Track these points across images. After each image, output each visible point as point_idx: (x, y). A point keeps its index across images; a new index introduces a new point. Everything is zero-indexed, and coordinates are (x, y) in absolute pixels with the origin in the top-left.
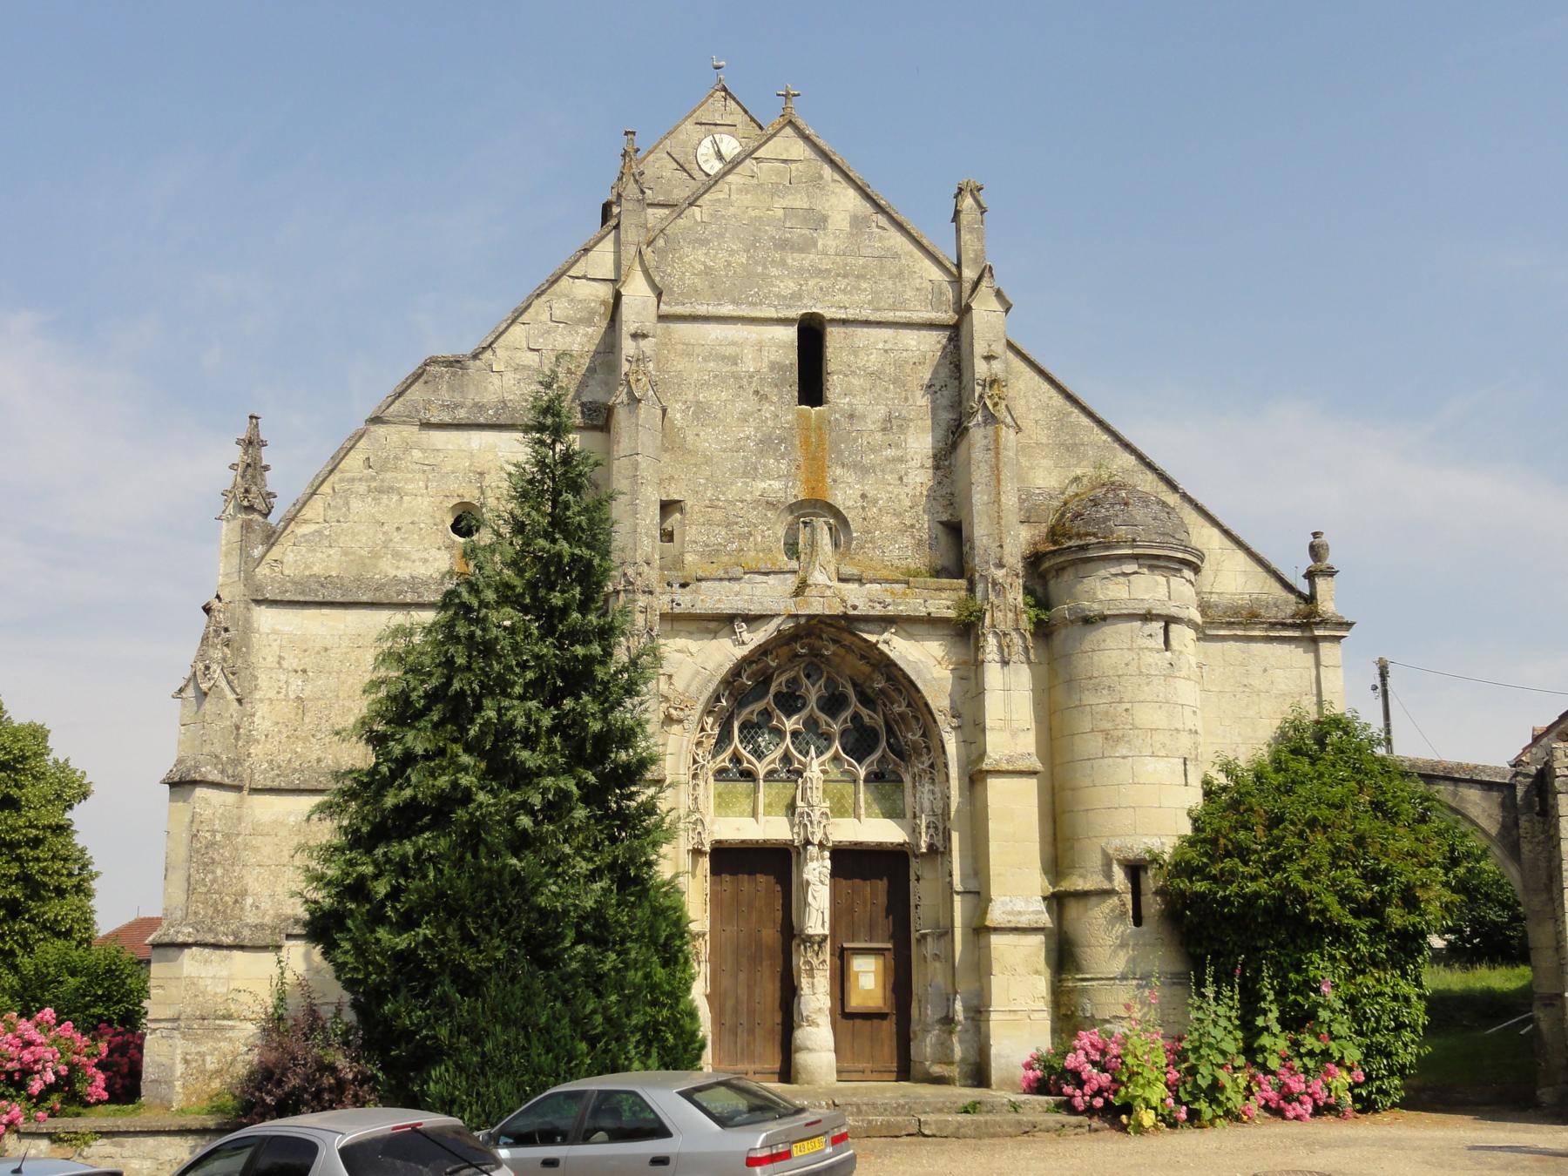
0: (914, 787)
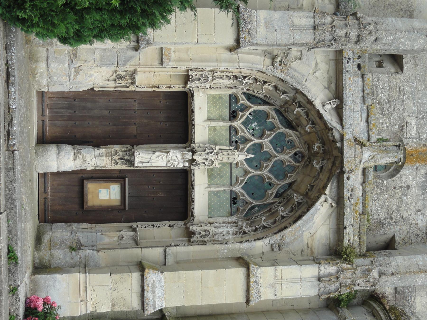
0: (229, 223)
